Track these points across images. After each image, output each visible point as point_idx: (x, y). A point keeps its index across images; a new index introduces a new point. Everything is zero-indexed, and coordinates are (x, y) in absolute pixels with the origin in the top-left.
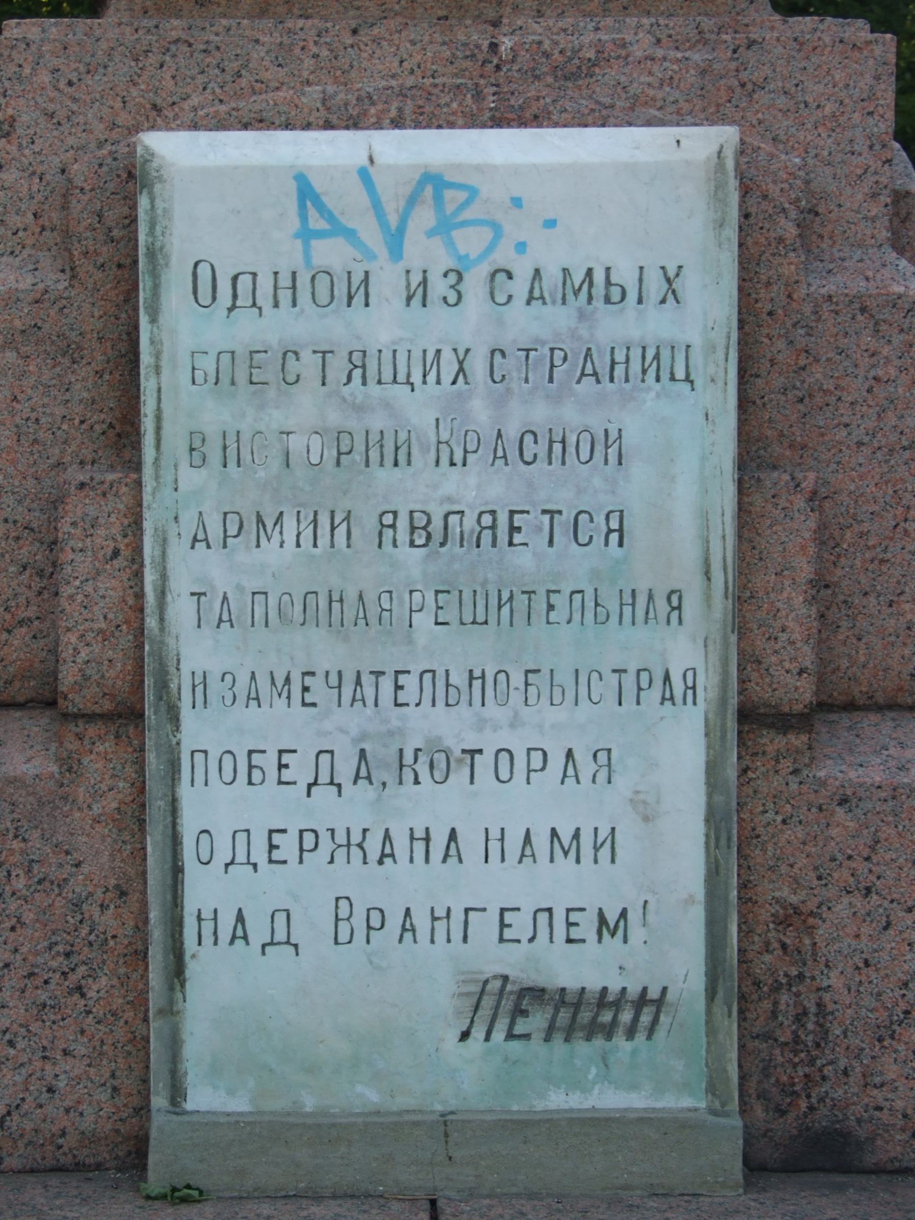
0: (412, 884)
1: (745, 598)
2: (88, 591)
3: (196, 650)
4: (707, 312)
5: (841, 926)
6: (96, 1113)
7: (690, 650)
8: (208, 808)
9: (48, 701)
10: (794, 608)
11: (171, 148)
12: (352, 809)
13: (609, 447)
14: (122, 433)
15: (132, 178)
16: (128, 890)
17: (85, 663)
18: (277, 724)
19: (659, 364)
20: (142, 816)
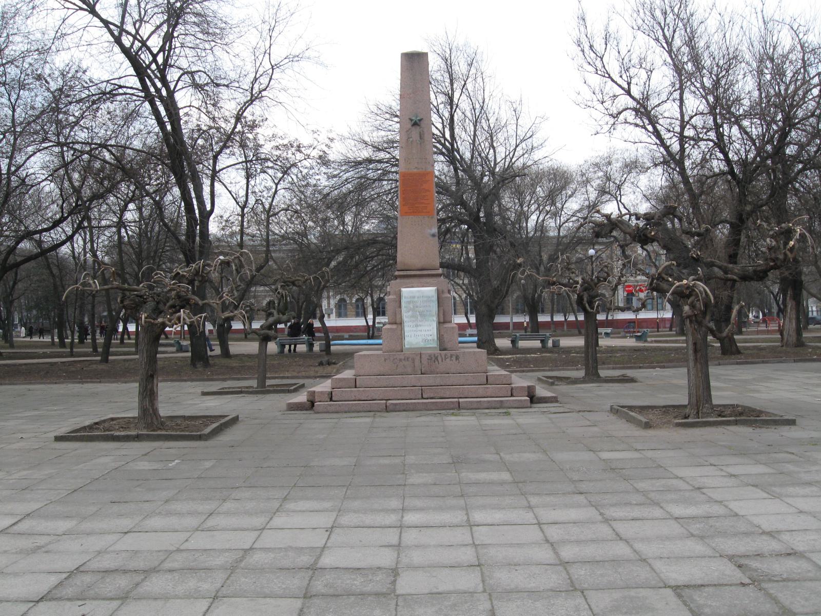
0: (419, 333)
1: (438, 315)
2: (398, 317)
3: (405, 319)
4: (435, 298)
5: (445, 336)
6: (399, 349)
7: (435, 318)
8: (406, 329)
9: (396, 323)
10: (442, 316)
11: (403, 290)
12: (415, 329)
13: (430, 306)
14: (400, 307)
15: (400, 291)
16: (401, 335)
17: (398, 321)
18: (410, 324)
19: (433, 301)
20: (402, 330)
